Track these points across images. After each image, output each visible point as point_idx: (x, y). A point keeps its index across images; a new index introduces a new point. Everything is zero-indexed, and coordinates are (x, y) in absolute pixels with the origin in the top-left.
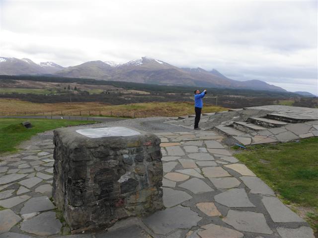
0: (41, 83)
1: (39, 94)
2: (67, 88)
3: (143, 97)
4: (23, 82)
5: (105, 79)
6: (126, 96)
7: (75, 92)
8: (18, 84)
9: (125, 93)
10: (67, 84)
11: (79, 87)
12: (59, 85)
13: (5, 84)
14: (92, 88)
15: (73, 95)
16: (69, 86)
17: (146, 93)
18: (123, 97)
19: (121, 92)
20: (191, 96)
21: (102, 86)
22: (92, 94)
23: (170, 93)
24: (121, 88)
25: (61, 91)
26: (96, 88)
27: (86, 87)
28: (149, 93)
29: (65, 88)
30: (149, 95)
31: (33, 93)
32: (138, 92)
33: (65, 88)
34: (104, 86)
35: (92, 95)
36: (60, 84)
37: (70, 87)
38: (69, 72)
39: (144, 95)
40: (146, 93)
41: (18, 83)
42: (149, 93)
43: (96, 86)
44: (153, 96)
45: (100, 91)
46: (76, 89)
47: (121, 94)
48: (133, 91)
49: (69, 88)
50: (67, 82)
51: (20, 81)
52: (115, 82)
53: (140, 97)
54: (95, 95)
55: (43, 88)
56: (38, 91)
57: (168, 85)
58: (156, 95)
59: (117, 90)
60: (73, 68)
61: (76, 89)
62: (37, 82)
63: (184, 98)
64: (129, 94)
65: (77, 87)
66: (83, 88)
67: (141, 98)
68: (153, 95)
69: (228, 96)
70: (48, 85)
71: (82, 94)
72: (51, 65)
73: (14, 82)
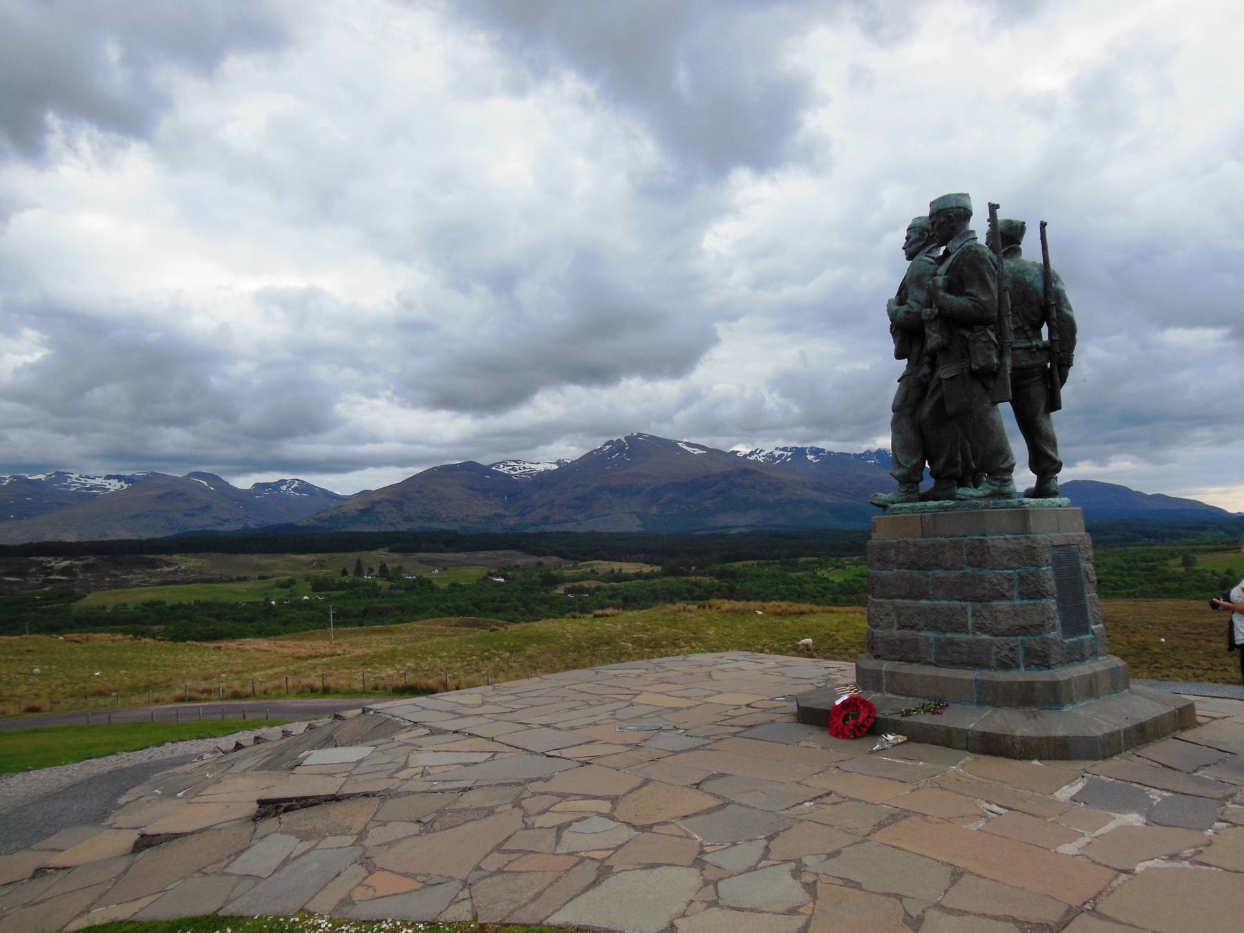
0: (256, 559)
1: (233, 599)
2: (351, 571)
4: (189, 562)
5: (496, 529)
6: (569, 585)
8: (166, 569)
9: (567, 573)
10: (352, 556)
11: (395, 565)
13: (117, 572)
16: (359, 562)
17: (647, 569)
20: (821, 565)
21: (481, 554)
22: (444, 585)
24: (555, 559)
26: (458, 564)
27: (421, 561)
29: (344, 573)
30: (657, 575)
31: (224, 598)
32: (616, 566)
33: (344, 573)
38: (363, 512)
39: (639, 576)
40: (647, 569)
41: (169, 564)
42: (657, 569)
43: (461, 556)
46: (383, 571)
47: (553, 581)
48: (604, 566)
49: (359, 571)
50: (352, 550)
51: (177, 557)
53: (622, 584)
55: (261, 578)
56: (240, 593)
57: (733, 531)
60: (378, 498)
62: (241, 558)
65: (389, 566)
70: (283, 565)
72: (295, 490)
73: (153, 564)
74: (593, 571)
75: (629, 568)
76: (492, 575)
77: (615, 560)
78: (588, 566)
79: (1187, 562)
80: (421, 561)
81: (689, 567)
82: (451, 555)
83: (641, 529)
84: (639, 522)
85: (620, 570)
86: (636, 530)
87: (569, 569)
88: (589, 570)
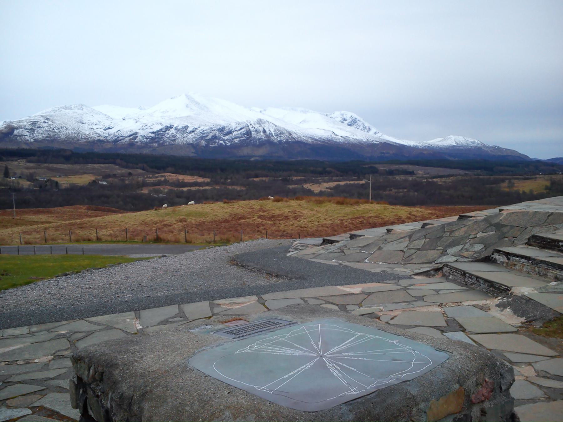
3: (193, 189)
7: (25, 184)
14: (66, 173)
15: (18, 190)
17: (200, 180)
18: (145, 191)
20: (306, 181)
21: (90, 166)
23: (257, 176)
24: (140, 171)
27: (49, 169)
28: (208, 180)
30: (208, 184)
32: (181, 177)
35: (67, 190)
37: (10, 171)
39: (196, 184)
40: (200, 180)
42: (208, 180)
43: (77, 166)
44: (217, 187)
52: (125, 155)
53: (185, 189)
57: (252, 159)
58: (223, 184)
59: (130, 174)
63: (291, 187)
64: (159, 183)
67: (189, 191)
68: (217, 183)
69: (391, 177)
71: (41, 187)
74: (165, 179)
75: (188, 179)
76: (98, 180)
77: (179, 174)
78: (162, 176)
79: (511, 185)
80: (49, 169)
82: (69, 166)
83: (195, 155)
84: (193, 151)
85: (183, 179)
86: (192, 155)
88: (163, 179)
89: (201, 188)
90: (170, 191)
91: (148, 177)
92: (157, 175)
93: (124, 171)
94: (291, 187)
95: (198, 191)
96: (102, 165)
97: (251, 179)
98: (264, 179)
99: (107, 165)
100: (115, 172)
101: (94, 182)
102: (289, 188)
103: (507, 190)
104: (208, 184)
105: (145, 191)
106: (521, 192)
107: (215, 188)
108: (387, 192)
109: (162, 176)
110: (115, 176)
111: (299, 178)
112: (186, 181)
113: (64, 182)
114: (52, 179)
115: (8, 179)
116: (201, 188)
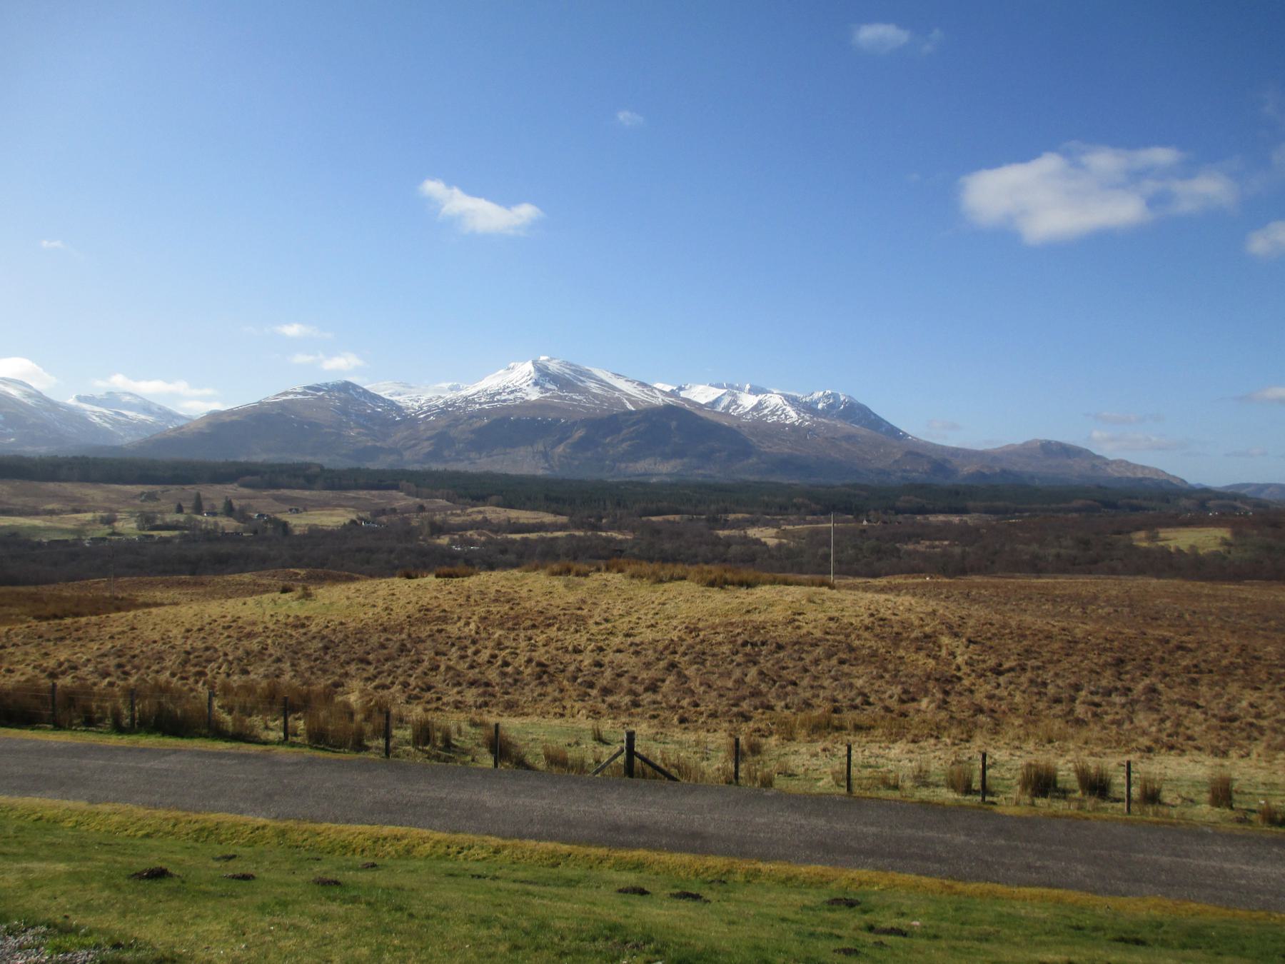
2: (188, 505)
3: (533, 536)
5: (373, 465)
9: (455, 520)
10: (191, 490)
11: (243, 502)
12: (151, 497)
17: (548, 518)
19: (438, 518)
20: (754, 523)
21: (351, 494)
25: (158, 522)
26: (323, 505)
27: (277, 499)
32: (514, 514)
34: (363, 493)
35: (303, 537)
36: (157, 488)
40: (548, 518)
45: (333, 519)
53: (517, 537)
54: (316, 534)
57: (654, 480)
61: (229, 510)
62: (52, 486)
63: (722, 533)
66: (262, 503)
71: (255, 532)
75: (525, 516)
78: (480, 512)
80: (277, 499)
81: (601, 518)
86: (540, 472)
87: (459, 515)
88: (480, 517)
89: (549, 535)
90: (490, 542)
91: (452, 514)
92: (470, 510)
93: (413, 501)
94: (722, 533)
95: (543, 540)
96: (374, 492)
97: (644, 519)
98: (671, 517)
99: (382, 492)
100: (396, 505)
101: (353, 522)
102: (717, 537)
103: (1145, 544)
104: (562, 527)
105: (444, 540)
106: (1172, 550)
107: (573, 536)
108: (910, 547)
109: (480, 512)
110: (394, 511)
111: (740, 516)
112: (521, 521)
113: (299, 522)
114: (279, 516)
115: (199, 517)
116: (549, 535)
